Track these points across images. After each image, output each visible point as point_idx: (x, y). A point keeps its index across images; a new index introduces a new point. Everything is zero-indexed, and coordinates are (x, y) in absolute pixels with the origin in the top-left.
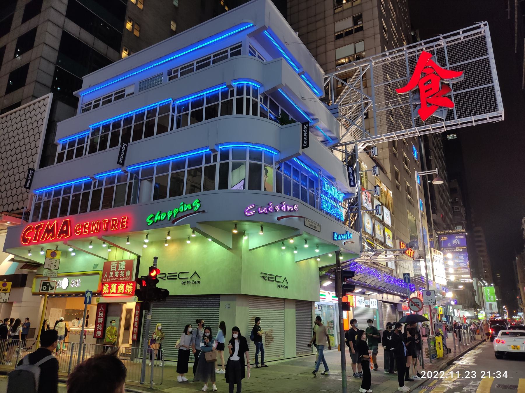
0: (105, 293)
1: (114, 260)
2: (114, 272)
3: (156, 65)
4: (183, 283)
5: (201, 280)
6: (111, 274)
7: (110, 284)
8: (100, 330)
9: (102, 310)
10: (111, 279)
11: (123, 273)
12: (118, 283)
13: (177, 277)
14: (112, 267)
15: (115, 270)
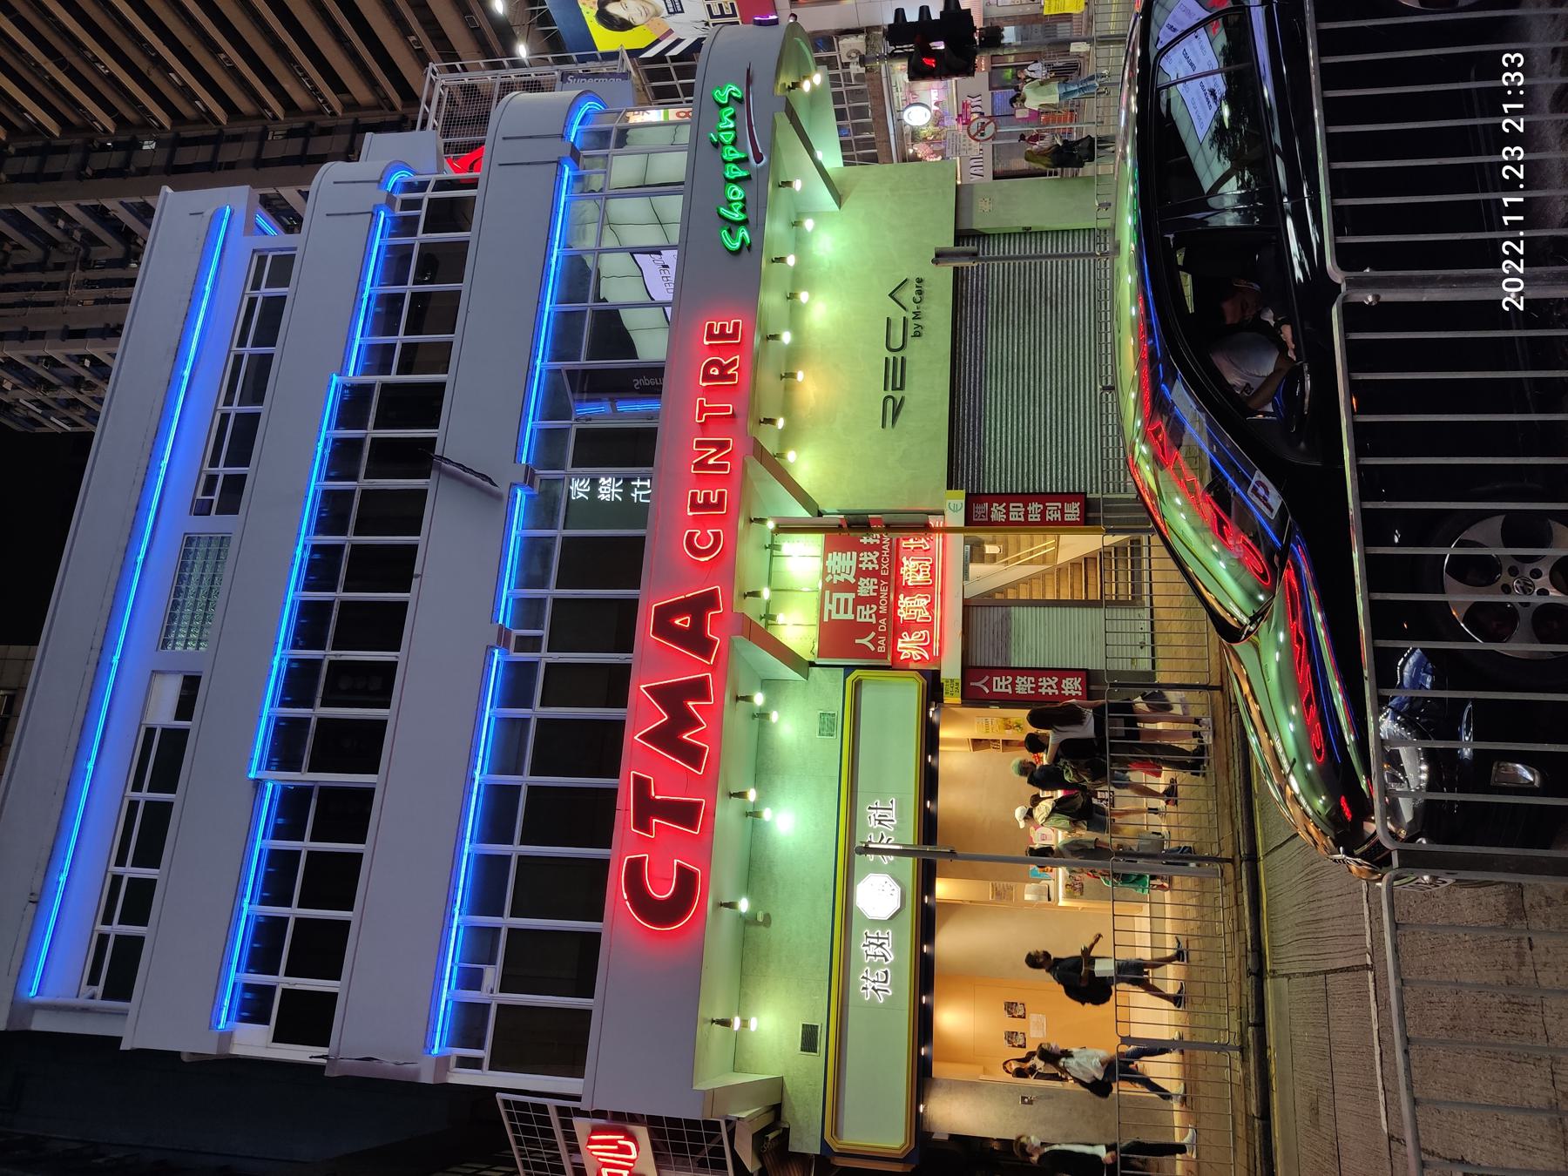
0: (929, 648)
1: (817, 565)
2: (859, 601)
3: (141, 557)
4: (917, 335)
5: (913, 277)
6: (866, 615)
7: (898, 628)
8: (1059, 684)
9: (989, 684)
10: (883, 610)
11: (865, 556)
12: (899, 587)
13: (899, 355)
14: (842, 616)
15: (851, 596)
